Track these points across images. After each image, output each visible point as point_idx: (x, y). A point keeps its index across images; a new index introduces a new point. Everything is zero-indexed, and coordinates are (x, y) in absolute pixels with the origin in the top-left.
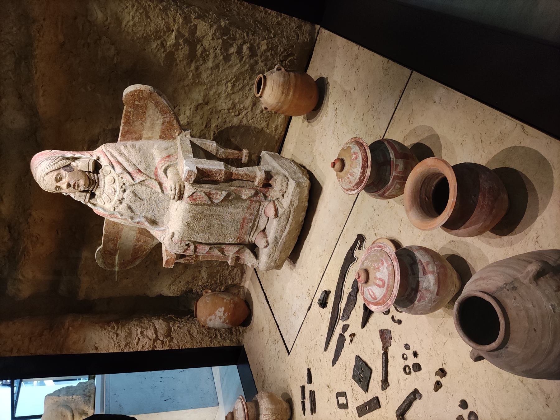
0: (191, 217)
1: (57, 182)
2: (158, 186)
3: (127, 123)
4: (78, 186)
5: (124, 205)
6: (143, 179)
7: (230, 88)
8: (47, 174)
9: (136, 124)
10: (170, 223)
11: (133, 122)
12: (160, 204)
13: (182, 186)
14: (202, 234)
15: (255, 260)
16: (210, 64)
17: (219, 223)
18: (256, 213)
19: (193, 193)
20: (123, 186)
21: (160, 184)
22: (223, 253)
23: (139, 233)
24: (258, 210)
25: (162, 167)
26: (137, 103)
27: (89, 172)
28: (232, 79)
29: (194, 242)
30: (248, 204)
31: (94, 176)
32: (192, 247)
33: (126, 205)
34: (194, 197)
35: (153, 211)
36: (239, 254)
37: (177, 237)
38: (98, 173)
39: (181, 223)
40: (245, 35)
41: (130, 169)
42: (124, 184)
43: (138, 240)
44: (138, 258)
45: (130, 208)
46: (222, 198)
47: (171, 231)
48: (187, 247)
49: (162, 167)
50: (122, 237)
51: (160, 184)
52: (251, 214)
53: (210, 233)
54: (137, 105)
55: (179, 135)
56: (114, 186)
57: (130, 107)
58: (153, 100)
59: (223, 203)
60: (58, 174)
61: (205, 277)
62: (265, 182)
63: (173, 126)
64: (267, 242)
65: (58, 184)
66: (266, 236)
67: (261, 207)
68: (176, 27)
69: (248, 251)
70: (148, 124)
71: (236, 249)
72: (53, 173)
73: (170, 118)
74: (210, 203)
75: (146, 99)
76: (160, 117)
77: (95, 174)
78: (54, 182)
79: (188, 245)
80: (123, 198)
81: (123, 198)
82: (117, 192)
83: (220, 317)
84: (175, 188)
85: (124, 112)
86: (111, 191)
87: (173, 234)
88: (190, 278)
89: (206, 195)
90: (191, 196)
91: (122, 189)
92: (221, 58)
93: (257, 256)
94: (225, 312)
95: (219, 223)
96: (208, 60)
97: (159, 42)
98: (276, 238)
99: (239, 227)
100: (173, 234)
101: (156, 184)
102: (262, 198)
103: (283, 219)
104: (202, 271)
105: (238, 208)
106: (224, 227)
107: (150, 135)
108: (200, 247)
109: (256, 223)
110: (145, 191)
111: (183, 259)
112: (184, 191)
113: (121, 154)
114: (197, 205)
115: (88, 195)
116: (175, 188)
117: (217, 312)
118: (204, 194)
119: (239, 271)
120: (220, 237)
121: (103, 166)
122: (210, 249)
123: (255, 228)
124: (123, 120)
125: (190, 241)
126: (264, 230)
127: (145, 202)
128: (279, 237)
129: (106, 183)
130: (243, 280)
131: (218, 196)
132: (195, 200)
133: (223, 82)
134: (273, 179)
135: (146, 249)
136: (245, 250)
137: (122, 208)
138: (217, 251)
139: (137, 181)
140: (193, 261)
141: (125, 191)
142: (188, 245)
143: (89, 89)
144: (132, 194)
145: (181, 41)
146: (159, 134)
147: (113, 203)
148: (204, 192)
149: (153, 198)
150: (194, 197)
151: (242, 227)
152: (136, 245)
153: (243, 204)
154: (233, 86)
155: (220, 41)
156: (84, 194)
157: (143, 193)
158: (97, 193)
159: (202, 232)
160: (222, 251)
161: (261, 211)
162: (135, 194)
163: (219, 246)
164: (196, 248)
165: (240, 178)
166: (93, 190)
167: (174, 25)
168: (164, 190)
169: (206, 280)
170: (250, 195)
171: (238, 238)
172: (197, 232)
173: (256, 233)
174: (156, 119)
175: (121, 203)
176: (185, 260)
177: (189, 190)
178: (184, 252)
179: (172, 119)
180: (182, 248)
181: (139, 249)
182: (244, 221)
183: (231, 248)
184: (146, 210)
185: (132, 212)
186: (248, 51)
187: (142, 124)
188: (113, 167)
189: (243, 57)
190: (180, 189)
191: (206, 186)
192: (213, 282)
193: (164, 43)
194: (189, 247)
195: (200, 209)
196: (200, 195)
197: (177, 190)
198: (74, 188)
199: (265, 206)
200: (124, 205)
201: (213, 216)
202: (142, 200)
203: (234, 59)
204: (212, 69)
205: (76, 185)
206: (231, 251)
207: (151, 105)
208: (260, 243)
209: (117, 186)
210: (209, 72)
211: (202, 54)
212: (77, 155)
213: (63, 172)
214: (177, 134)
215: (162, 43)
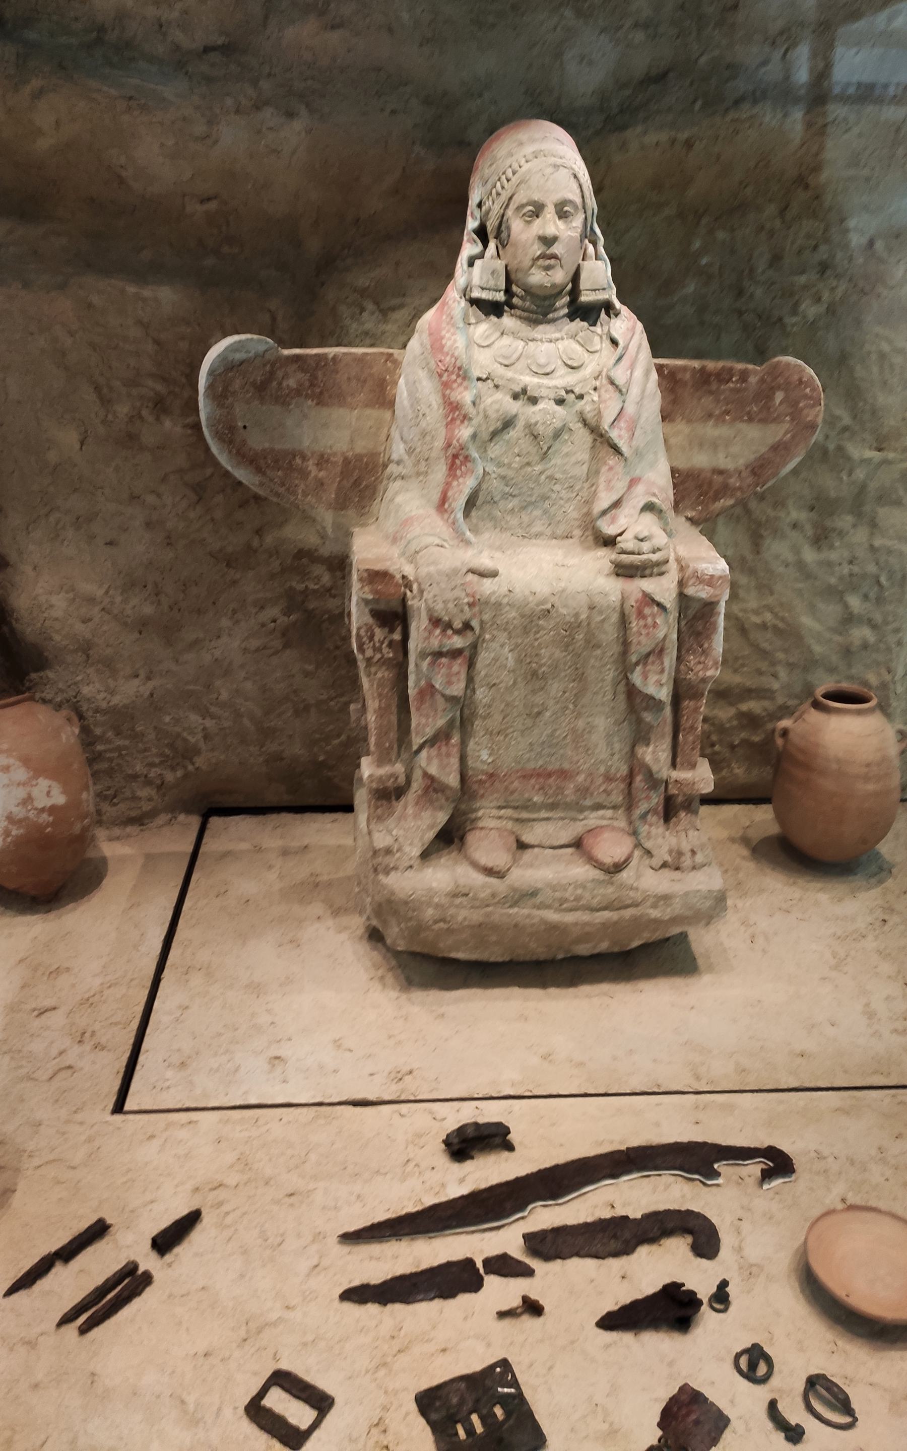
0: (577, 615)
1: (556, 206)
2: (615, 497)
3: (704, 379)
4: (548, 268)
5: (514, 407)
6: (624, 449)
7: (756, 620)
8: (575, 176)
9: (707, 401)
10: (498, 555)
11: (711, 393)
12: (537, 513)
13: (663, 569)
14: (511, 663)
15: (416, 851)
16: (810, 555)
17: (551, 703)
18: (588, 802)
19: (659, 605)
20: (572, 396)
21: (617, 504)
22: (432, 742)
23: (346, 461)
24: (598, 807)
25: (654, 495)
26: (779, 396)
27: (575, 292)
28: (783, 619)
29: (474, 647)
30: (618, 770)
31: (563, 307)
32: (458, 642)
33: (514, 412)
34: (647, 611)
35: (507, 496)
36: (426, 790)
37: (487, 586)
38: (572, 317)
39: (543, 589)
40: (894, 625)
41: (630, 409)
42: (581, 397)
43: (323, 460)
44: (259, 470)
45: (508, 423)
46: (651, 689)
47: (485, 561)
48: (457, 624)
49: (654, 495)
50: (325, 411)
51: (617, 504)
52: (584, 791)
53: (515, 683)
54: (770, 397)
55: (688, 519)
56: (563, 370)
57: (762, 381)
58: (793, 437)
59: (622, 697)
60: (576, 207)
61: (116, 700)
62: (680, 799)
63: (716, 498)
64: (509, 869)
65: (549, 212)
66: (515, 860)
67: (609, 813)
68: (891, 455)
69: (442, 818)
70: (710, 430)
71: (453, 780)
72: (578, 191)
73: (740, 488)
74: (634, 659)
75: (792, 420)
76: (741, 462)
77: (566, 311)
78: (557, 197)
79: (467, 626)
80: (534, 401)
81: (534, 401)
82: (545, 381)
83: (28, 800)
84: (659, 550)
85: (740, 366)
86: (542, 361)
87: (494, 574)
88: (109, 651)
89: (657, 644)
90: (649, 600)
91: (563, 393)
92: (833, 581)
93: (425, 855)
94: (52, 810)
95: (551, 703)
96: (819, 549)
97: (847, 420)
98: (534, 894)
99: (532, 765)
100: (494, 574)
101: (620, 486)
102: (643, 807)
103: (610, 891)
104: (136, 682)
105: (610, 744)
106: (529, 722)
107: (673, 441)
108: (459, 666)
109: (543, 814)
110: (573, 459)
111: (370, 620)
112: (651, 575)
113: (647, 373)
114: (624, 621)
115: (500, 297)
116: (659, 550)
117: (44, 783)
118: (661, 635)
119: (146, 807)
120: (498, 717)
121: (598, 329)
122: (452, 700)
123: (525, 815)
124: (711, 365)
125: (482, 628)
126: (522, 846)
127: (538, 468)
128: (539, 899)
129: (560, 345)
130: (117, 831)
131: (656, 678)
132: (640, 615)
133: (770, 600)
134: (693, 818)
135: (294, 493)
136: (441, 808)
137: (499, 403)
138: (441, 722)
139: (614, 434)
140: (369, 653)
141: (560, 402)
142: (467, 626)
143: (704, 261)
144: (558, 424)
145: (860, 474)
146: (682, 465)
147: (509, 374)
148: (665, 636)
149: (557, 488)
150: (647, 611)
151: (526, 776)
152: (304, 458)
153: (616, 757)
154: (764, 626)
155: (872, 568)
156: (504, 287)
157: (567, 455)
158: (508, 321)
159: (519, 661)
160: (439, 738)
161: (593, 819)
162: (557, 434)
163: (458, 723)
164: (455, 654)
165: (685, 722)
166: (512, 307)
167: (895, 450)
168: (608, 516)
169: (104, 705)
170: (655, 768)
171: (492, 775)
172: (517, 646)
173: (510, 825)
174: (735, 449)
175: (516, 397)
176: (370, 629)
177: (664, 588)
178: (436, 622)
179: (739, 494)
180: (455, 610)
181: (291, 468)
182: (549, 775)
183: (455, 761)
184: (511, 473)
185: (494, 434)
186: (857, 643)
187: (710, 416)
188: (620, 359)
189: (841, 634)
190: (658, 564)
191: (675, 636)
192: (98, 731)
193: (847, 434)
194: (458, 632)
195: (609, 634)
196: (655, 625)
197: (655, 557)
198: (543, 256)
199: (616, 824)
200: (514, 407)
201: (580, 677)
202: (544, 456)
203: (831, 611)
204: (801, 565)
205: (552, 262)
206: (442, 767)
207: (778, 432)
208: (488, 844)
209: (563, 379)
210: (790, 557)
211: (834, 530)
212: (602, 250)
213: (578, 222)
214: (690, 514)
215: (846, 429)
